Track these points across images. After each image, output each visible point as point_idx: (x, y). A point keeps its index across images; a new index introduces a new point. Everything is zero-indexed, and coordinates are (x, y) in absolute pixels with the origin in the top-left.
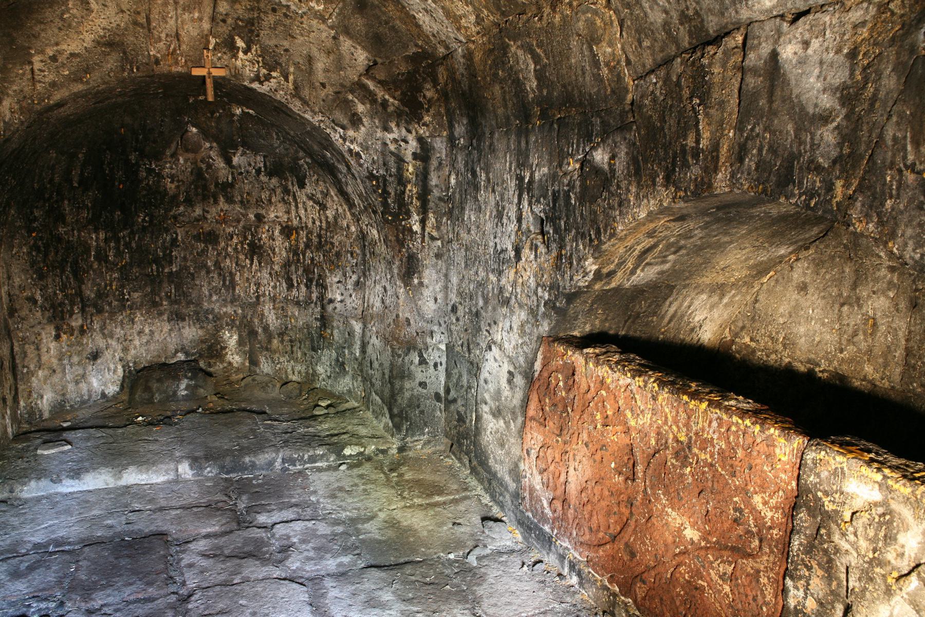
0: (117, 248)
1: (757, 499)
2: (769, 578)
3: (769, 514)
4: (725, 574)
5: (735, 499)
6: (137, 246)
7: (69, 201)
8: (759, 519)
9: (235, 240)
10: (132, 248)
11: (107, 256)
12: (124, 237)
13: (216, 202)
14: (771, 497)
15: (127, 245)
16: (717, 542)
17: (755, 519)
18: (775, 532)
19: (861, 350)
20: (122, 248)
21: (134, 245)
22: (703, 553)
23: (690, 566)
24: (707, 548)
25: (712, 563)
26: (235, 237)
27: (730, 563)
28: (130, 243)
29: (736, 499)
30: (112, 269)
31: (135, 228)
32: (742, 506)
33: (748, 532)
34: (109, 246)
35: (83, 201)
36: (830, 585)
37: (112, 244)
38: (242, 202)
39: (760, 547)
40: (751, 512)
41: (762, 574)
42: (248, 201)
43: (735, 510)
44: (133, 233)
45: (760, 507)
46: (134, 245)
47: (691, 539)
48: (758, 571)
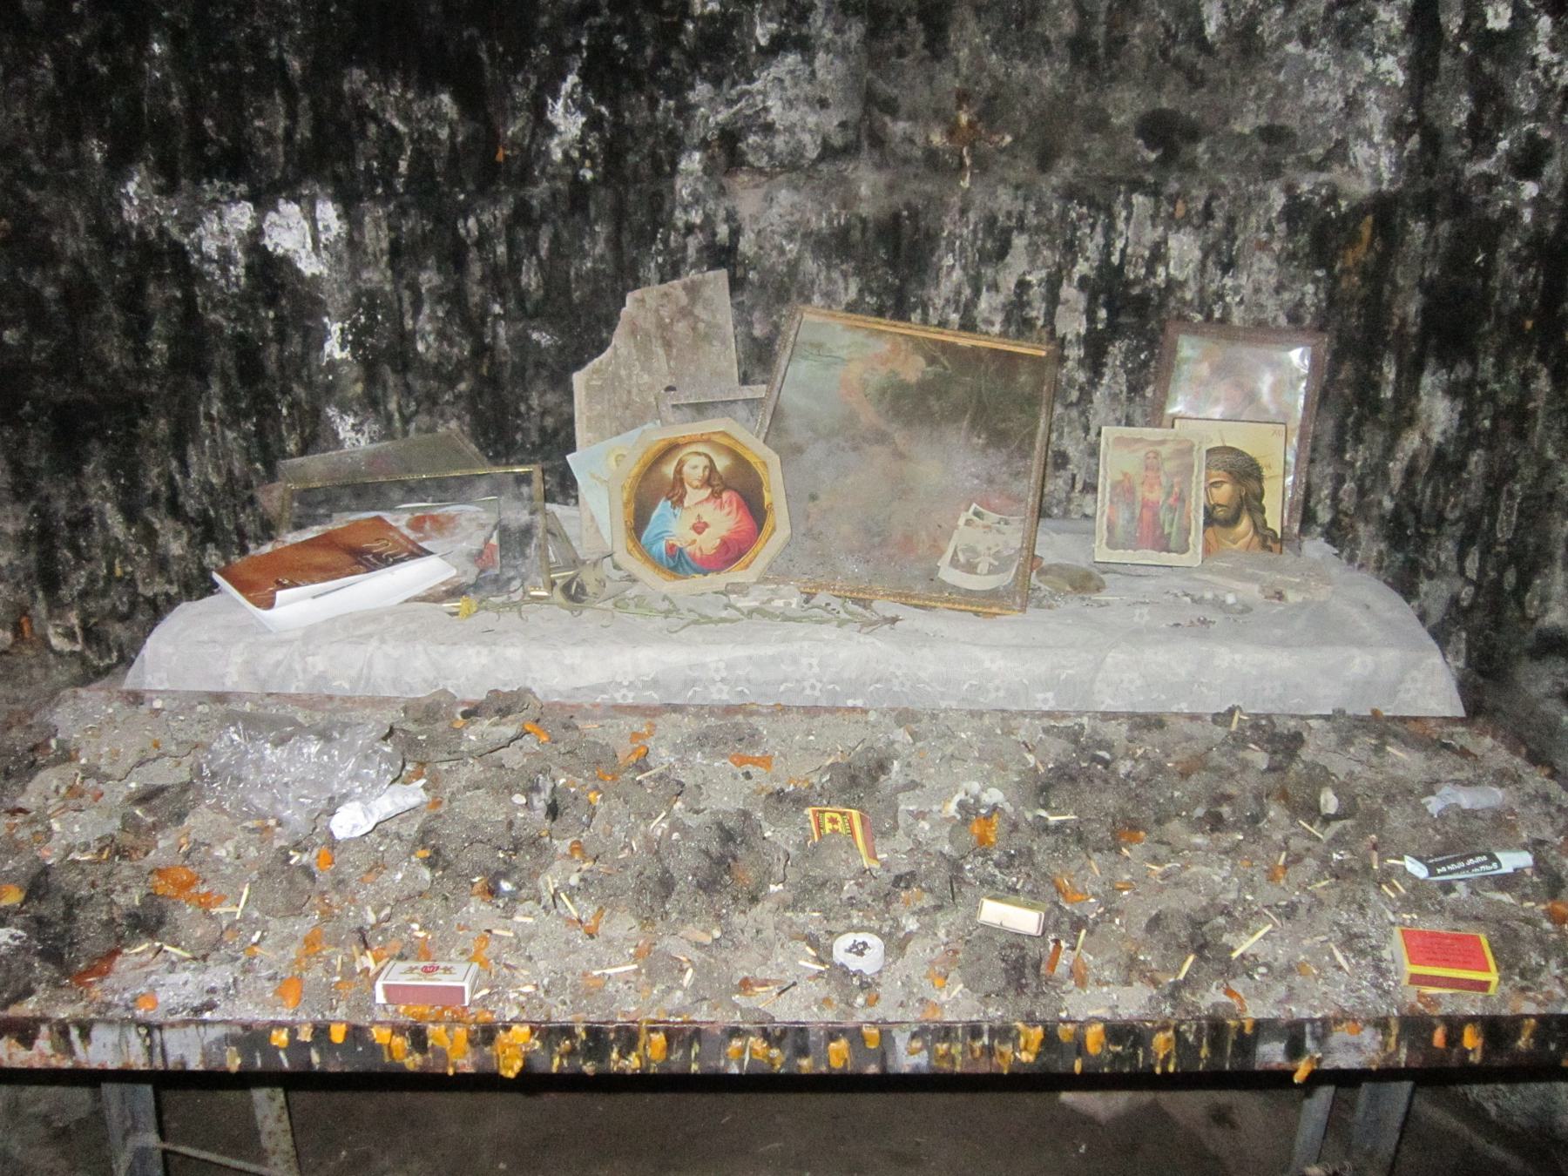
0: (455, 298)
6: (547, 283)
7: (177, 38)
9: (1018, 263)
10: (522, 296)
11: (406, 338)
12: (484, 240)
13: (937, 47)
15: (501, 279)
20: (475, 293)
21: (530, 279)
26: (1020, 241)
28: (514, 267)
30: (432, 399)
31: (539, 193)
34: (414, 287)
35: (257, 46)
37: (429, 278)
38: (1079, 46)
42: (1117, 43)
44: (522, 216)
46: (530, 279)
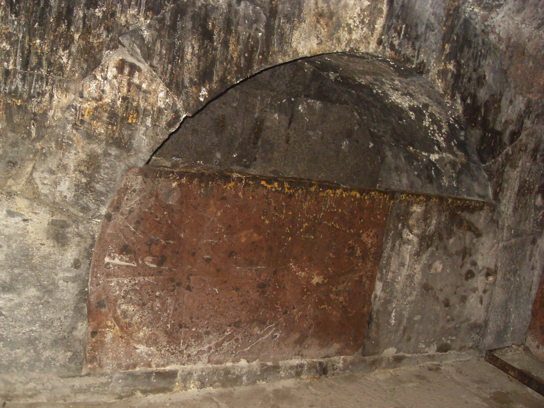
1: (364, 237)
3: (370, 242)
5: (349, 242)
18: (372, 249)
19: (213, 143)
41: (364, 277)
43: (349, 249)
47: (317, 283)
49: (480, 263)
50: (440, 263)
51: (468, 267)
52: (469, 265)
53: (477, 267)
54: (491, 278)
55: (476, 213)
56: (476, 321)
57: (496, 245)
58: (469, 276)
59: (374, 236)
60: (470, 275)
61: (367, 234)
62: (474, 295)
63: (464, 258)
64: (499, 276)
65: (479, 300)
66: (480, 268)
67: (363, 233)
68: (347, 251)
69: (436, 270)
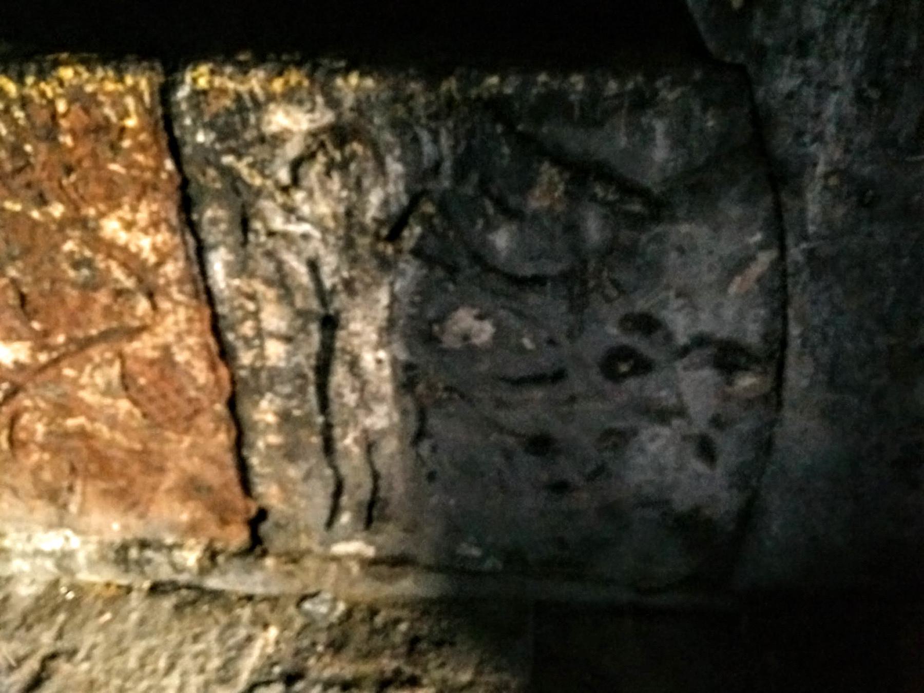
1: (111, 227)
2: (190, 348)
4: (109, 384)
8: (129, 260)
14: (134, 209)
16: (70, 340)
17: (124, 265)
22: (51, 372)
23: (36, 408)
24: (55, 362)
25: (74, 382)
27: (110, 363)
29: (69, 246)
32: (88, 253)
33: (119, 293)
36: (292, 304)
39: (154, 307)
40: (109, 256)
41: (175, 349)
45: (123, 237)
47: (16, 363)
48: (166, 349)
49: (680, 325)
50: (480, 317)
51: (613, 333)
52: (613, 331)
53: (658, 335)
54: (746, 381)
55: (621, 121)
56: (697, 509)
57: (765, 259)
58: (624, 368)
59: (155, 224)
60: (620, 363)
61: (121, 219)
62: (665, 431)
63: (578, 303)
64: (798, 375)
65: (691, 448)
66: (682, 339)
67: (102, 215)
68: (72, 273)
69: (466, 337)
